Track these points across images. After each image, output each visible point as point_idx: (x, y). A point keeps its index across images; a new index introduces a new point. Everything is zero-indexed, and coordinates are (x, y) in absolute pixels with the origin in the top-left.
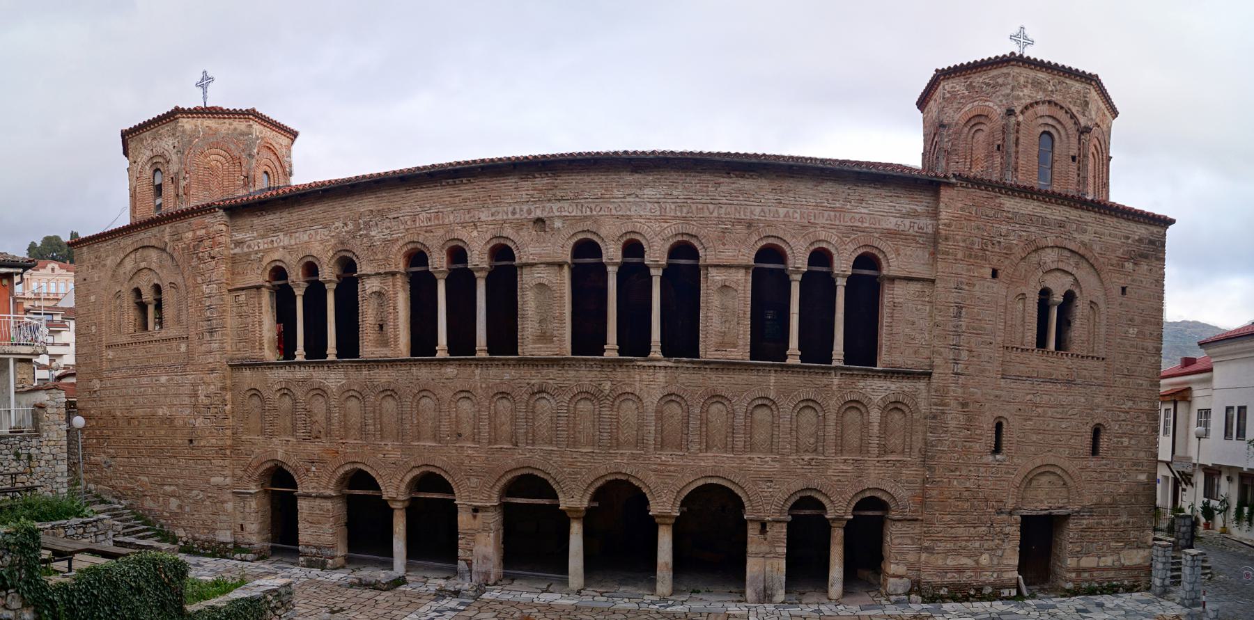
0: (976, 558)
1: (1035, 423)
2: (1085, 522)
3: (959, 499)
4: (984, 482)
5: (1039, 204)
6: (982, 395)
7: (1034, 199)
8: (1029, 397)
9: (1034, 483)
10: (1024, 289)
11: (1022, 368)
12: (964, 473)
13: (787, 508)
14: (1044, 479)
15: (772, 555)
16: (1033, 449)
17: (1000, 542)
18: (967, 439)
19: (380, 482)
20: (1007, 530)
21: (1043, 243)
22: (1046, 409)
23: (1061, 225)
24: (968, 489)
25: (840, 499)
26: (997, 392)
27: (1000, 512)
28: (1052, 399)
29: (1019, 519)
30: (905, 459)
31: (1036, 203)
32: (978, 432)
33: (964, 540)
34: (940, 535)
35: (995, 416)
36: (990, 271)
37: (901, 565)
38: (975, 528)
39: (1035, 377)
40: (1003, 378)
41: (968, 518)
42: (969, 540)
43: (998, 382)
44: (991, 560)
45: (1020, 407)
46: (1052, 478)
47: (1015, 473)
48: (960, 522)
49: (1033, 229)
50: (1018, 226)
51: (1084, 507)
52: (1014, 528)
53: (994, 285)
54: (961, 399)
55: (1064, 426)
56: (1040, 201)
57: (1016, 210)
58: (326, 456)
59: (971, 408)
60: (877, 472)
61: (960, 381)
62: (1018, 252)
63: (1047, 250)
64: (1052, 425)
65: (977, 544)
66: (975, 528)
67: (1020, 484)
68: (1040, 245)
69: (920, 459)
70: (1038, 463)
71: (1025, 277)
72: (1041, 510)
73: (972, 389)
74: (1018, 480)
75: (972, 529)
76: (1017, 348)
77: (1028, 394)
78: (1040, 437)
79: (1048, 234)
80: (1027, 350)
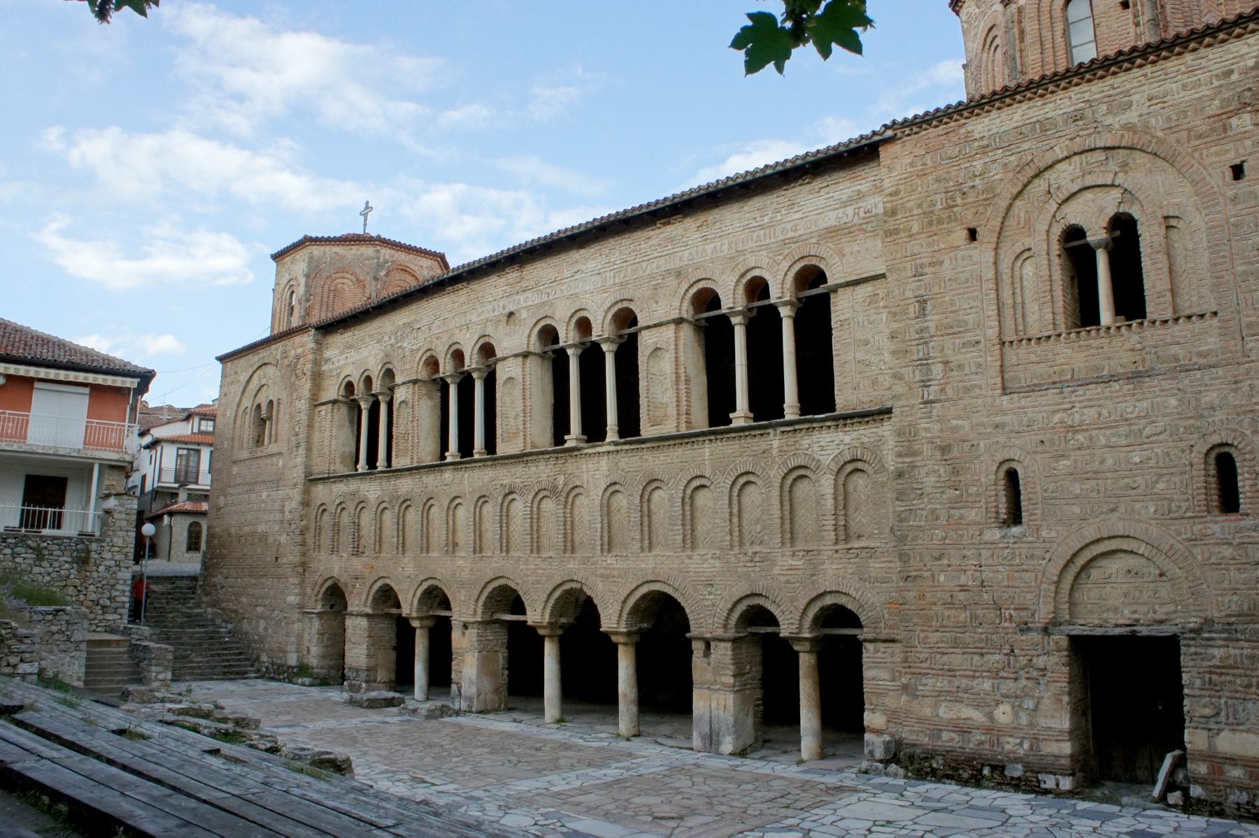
0: (987, 710)
1: (1076, 461)
2: (1216, 652)
3: (950, 604)
4: (991, 575)
5: (1031, 103)
6: (972, 428)
7: (1020, 102)
8: (1057, 418)
9: (1095, 574)
10: (1028, 242)
11: (1041, 369)
12: (955, 561)
13: (733, 621)
14: (1115, 566)
15: (718, 687)
16: (1077, 510)
17: (1030, 684)
18: (955, 504)
19: (401, 597)
20: (1040, 662)
21: (1049, 158)
22: (1094, 433)
23: (1076, 118)
24: (964, 588)
25: (792, 608)
26: (998, 419)
27: (1025, 628)
28: (1105, 413)
29: (1064, 642)
30: (872, 545)
31: (1025, 105)
32: (973, 490)
33: (968, 677)
34: (925, 665)
35: (999, 458)
36: (965, 233)
37: (878, 715)
38: (982, 655)
39: (1067, 381)
40: (1006, 394)
41: (967, 637)
42: (974, 677)
43: (998, 401)
44: (1016, 715)
45: (1041, 437)
46: (1132, 561)
47: (1047, 556)
48: (956, 643)
49: (1025, 146)
50: (1001, 151)
51: (1209, 622)
52: (1054, 659)
53: (971, 252)
54: (938, 441)
55: (1137, 460)
56: (1030, 99)
57: (995, 131)
58: (366, 573)
59: (955, 452)
60: (834, 567)
61: (935, 412)
62: (1010, 190)
63: (1059, 166)
64: (1110, 462)
65: (987, 685)
66: (982, 655)
67: (1060, 576)
68: (1042, 165)
69: (893, 544)
70: (1090, 534)
71: (1028, 221)
72: (1117, 626)
73: (954, 422)
74: (1054, 571)
75: (976, 658)
76: (1030, 340)
77: (1054, 412)
78: (1088, 486)
79: (1053, 142)
80: (1049, 337)
